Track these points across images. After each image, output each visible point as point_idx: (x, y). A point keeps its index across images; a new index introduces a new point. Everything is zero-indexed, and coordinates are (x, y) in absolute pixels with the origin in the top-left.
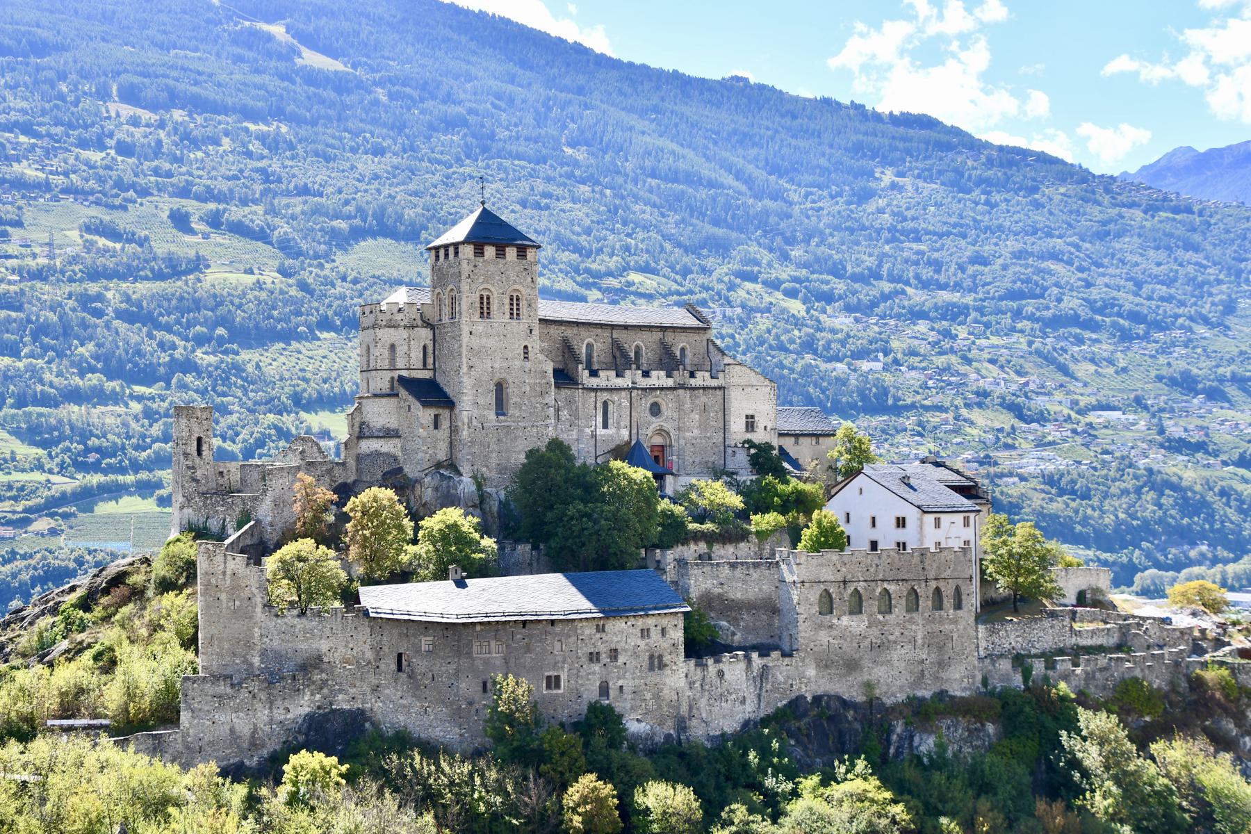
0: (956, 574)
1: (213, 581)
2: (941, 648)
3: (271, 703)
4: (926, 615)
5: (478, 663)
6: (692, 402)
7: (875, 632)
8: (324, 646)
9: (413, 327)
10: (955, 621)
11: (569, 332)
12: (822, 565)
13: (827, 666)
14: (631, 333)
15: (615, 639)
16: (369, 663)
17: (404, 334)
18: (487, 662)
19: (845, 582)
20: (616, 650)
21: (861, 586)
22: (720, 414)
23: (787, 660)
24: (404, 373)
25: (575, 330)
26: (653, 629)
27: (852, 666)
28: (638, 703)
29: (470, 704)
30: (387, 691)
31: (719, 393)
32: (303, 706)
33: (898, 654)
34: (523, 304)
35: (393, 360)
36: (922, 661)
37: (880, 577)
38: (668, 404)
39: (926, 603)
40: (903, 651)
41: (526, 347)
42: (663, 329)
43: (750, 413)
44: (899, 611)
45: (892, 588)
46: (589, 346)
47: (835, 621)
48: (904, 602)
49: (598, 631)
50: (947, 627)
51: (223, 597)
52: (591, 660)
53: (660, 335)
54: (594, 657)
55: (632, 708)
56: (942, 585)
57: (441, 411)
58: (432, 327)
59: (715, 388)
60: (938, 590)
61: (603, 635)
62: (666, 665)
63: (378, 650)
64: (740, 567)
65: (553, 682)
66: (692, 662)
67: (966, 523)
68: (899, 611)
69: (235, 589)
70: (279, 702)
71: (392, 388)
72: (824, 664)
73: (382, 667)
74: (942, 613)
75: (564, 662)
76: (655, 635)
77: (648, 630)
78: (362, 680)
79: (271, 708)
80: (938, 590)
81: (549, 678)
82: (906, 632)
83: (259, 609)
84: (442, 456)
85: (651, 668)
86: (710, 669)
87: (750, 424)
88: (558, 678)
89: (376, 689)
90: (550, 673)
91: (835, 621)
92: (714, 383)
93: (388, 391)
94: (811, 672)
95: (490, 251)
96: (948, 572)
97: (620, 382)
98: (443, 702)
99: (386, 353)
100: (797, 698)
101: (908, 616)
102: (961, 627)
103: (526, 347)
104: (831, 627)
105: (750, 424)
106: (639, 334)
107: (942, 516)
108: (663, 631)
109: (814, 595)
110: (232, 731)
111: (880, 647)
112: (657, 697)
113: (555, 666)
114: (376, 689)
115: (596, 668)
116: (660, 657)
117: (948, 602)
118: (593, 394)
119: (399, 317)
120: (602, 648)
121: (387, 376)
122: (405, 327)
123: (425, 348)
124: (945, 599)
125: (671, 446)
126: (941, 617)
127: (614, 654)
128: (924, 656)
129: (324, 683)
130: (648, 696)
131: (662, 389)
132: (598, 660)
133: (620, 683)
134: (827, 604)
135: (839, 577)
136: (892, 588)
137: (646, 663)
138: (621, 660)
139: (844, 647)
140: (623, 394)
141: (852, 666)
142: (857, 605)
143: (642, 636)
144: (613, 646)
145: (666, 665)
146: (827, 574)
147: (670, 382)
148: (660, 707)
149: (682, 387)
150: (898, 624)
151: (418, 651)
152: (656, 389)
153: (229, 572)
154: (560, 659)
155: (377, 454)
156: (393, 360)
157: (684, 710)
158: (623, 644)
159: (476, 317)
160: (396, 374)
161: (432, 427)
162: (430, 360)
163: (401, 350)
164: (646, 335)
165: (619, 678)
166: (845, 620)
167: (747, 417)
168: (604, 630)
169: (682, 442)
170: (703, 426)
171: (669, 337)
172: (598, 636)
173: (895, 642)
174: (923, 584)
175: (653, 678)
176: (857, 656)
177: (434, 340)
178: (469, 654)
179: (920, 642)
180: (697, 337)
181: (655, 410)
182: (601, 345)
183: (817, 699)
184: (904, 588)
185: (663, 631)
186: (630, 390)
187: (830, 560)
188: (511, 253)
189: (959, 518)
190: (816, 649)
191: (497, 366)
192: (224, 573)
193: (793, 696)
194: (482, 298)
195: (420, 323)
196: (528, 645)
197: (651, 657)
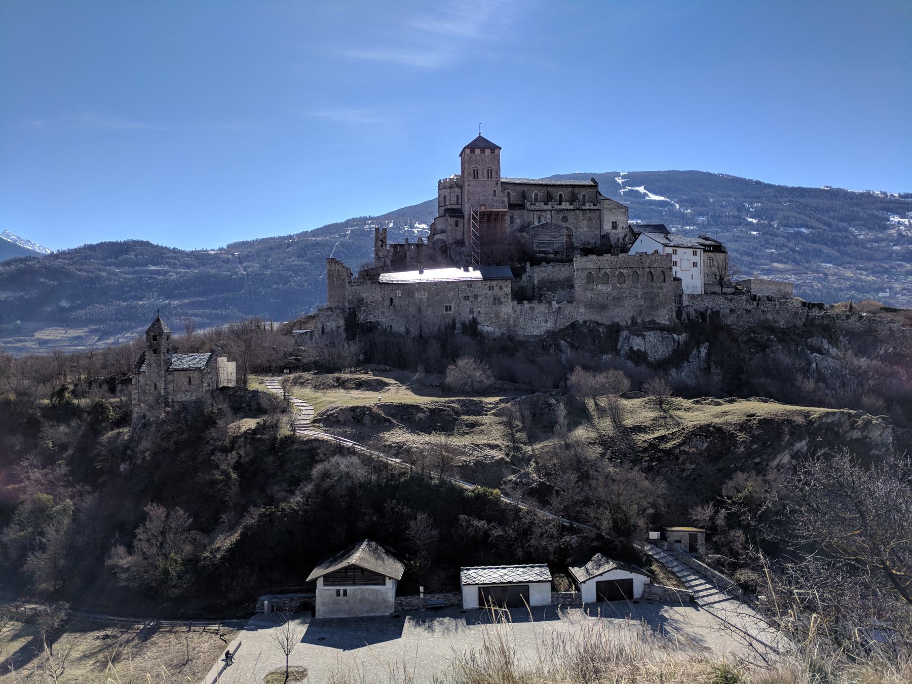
0: (661, 266)
2: (653, 300)
5: (417, 300)
6: (584, 216)
7: (616, 291)
8: (364, 295)
10: (661, 288)
11: (525, 189)
12: (587, 261)
14: (557, 189)
15: (476, 290)
17: (449, 190)
19: (599, 269)
21: (608, 271)
22: (598, 222)
23: (570, 305)
24: (449, 207)
25: (529, 187)
27: (603, 307)
29: (414, 317)
31: (598, 212)
33: (627, 303)
34: (494, 173)
36: (641, 306)
37: (618, 266)
38: (571, 217)
41: (495, 191)
42: (573, 186)
43: (614, 221)
45: (625, 271)
46: (536, 194)
47: (595, 287)
48: (631, 278)
49: (468, 287)
50: (655, 291)
51: (335, 279)
52: (465, 300)
53: (572, 189)
54: (466, 298)
56: (652, 270)
57: (458, 219)
58: (461, 188)
59: (595, 210)
60: (650, 272)
61: (471, 289)
62: (502, 303)
63: (383, 297)
65: (448, 308)
66: (516, 302)
67: (695, 253)
69: (339, 276)
71: (445, 214)
72: (590, 306)
74: (653, 284)
76: (496, 289)
77: (493, 287)
78: (378, 309)
81: (446, 307)
82: (632, 293)
83: (347, 284)
84: (459, 238)
85: (494, 304)
86: (525, 305)
87: (615, 225)
88: (450, 306)
89: (383, 313)
90: (447, 305)
91: (595, 287)
92: (595, 208)
94: (582, 310)
95: (478, 151)
97: (546, 207)
99: (443, 200)
100: (575, 322)
101: (634, 285)
102: (664, 291)
103: (495, 191)
104: (593, 289)
105: (615, 225)
106: (561, 189)
107: (678, 249)
108: (501, 288)
109: (584, 275)
110: (332, 329)
111: (618, 299)
112: (497, 316)
116: (499, 299)
118: (532, 213)
120: (470, 294)
121: (443, 209)
122: (449, 188)
123: (458, 196)
125: (572, 235)
126: (652, 285)
127: (476, 297)
128: (642, 303)
129: (365, 310)
130: (493, 316)
131: (567, 210)
133: (479, 310)
134: (590, 278)
135: (597, 266)
136: (625, 271)
137: (491, 300)
138: (479, 299)
139: (600, 299)
140: (547, 212)
141: (603, 307)
142: (605, 279)
143: (490, 290)
145: (502, 303)
146: (590, 265)
147: (572, 207)
148: (499, 321)
149: (578, 209)
151: (396, 296)
152: (564, 210)
153: (336, 270)
154: (451, 298)
155: (438, 240)
157: (511, 322)
159: (472, 179)
161: (454, 226)
162: (460, 201)
164: (564, 189)
165: (478, 307)
166: (600, 286)
167: (613, 222)
169: (578, 233)
170: (589, 226)
171: (576, 190)
173: (626, 297)
174: (642, 270)
177: (461, 193)
178: (413, 296)
179: (640, 297)
180: (591, 190)
181: (565, 219)
182: (541, 194)
183: (585, 322)
184: (631, 271)
185: (501, 288)
186: (551, 211)
187: (592, 259)
188: (488, 152)
190: (585, 300)
191: (481, 199)
193: (573, 321)
194: (474, 171)
195: (455, 186)
196: (438, 293)
197: (494, 299)
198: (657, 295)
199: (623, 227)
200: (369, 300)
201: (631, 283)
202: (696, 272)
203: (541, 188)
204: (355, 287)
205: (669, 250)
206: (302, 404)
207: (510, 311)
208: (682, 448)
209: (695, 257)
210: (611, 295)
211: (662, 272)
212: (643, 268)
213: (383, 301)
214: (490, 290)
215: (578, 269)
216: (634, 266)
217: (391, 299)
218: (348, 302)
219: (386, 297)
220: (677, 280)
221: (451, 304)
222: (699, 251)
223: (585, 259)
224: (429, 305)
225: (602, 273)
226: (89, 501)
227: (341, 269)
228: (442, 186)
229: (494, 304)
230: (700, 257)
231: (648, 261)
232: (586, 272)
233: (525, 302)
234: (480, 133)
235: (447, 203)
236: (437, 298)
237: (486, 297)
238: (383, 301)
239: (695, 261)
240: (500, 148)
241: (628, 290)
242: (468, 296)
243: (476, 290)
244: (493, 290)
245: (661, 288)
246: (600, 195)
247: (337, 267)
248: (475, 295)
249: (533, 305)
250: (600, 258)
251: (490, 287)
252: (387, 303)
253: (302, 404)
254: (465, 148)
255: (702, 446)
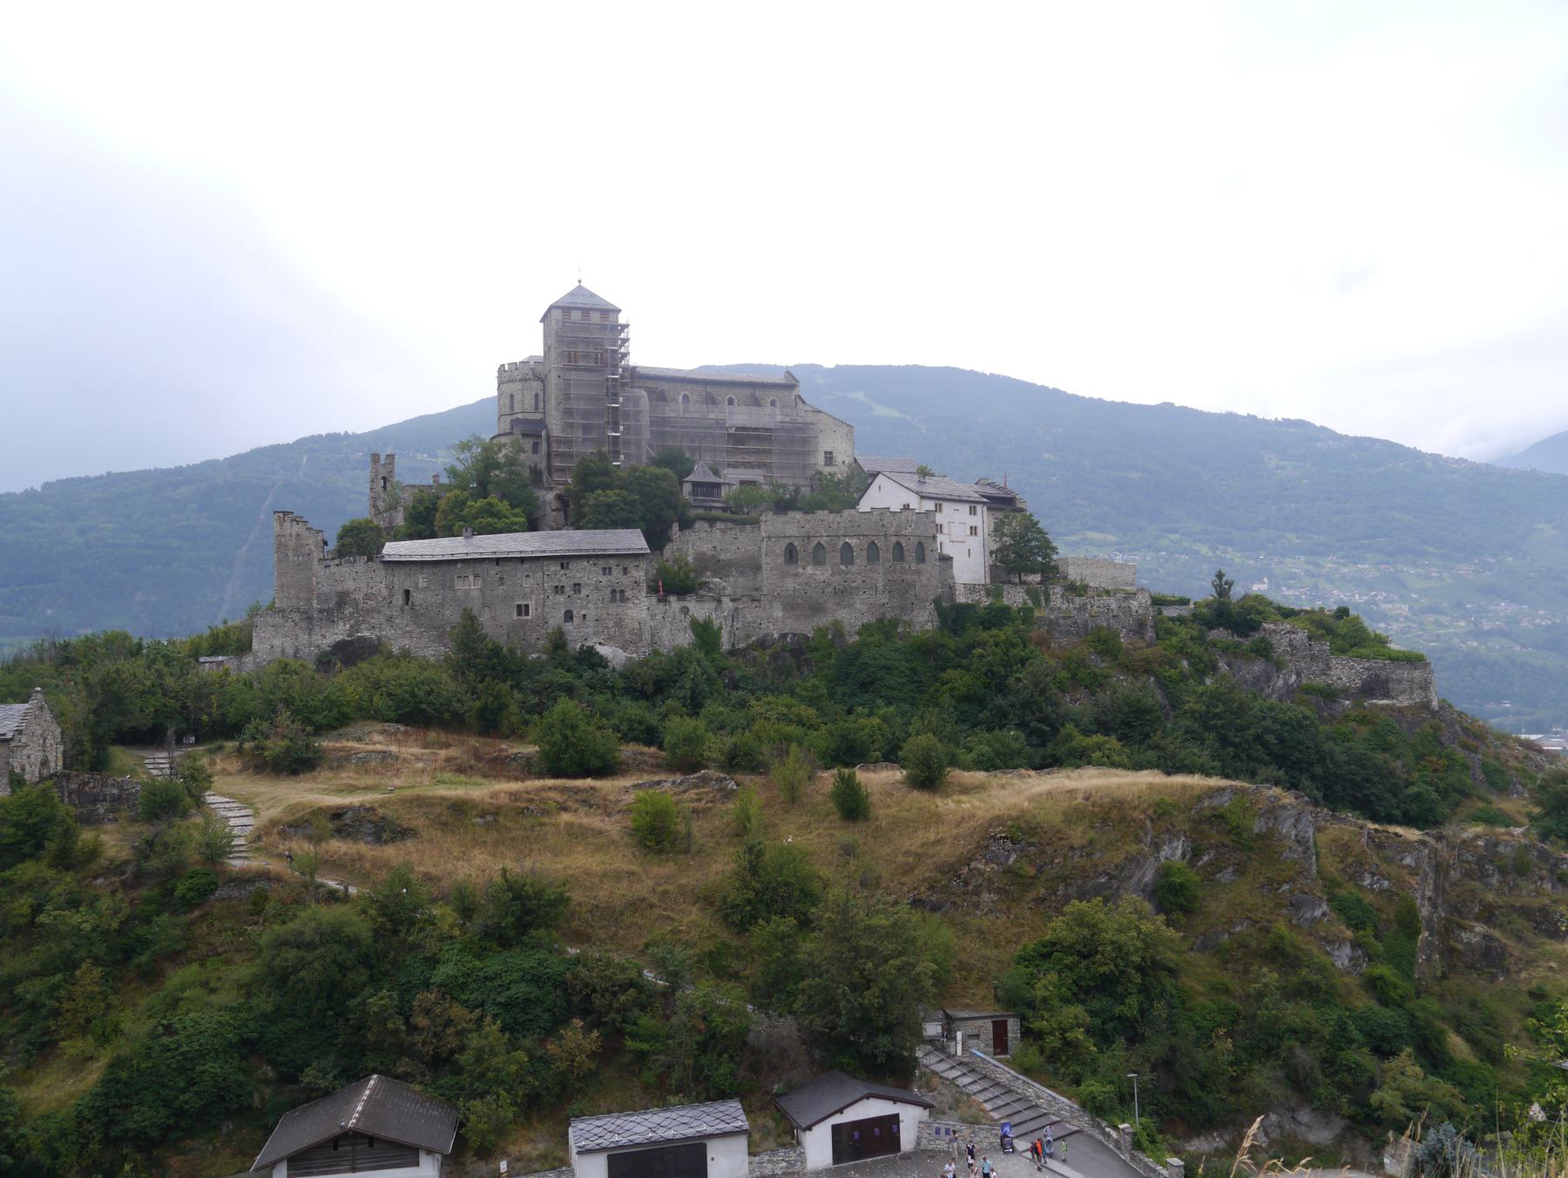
0: (919, 533)
1: (283, 541)
3: (311, 630)
4: (887, 565)
9: (526, 380)
10: (918, 572)
12: (786, 522)
13: (792, 609)
15: (578, 575)
16: (384, 599)
17: (519, 386)
18: (467, 593)
19: (808, 537)
20: (579, 584)
21: (824, 541)
23: (755, 603)
24: (520, 416)
26: (614, 567)
27: (817, 608)
28: (600, 629)
30: (397, 621)
32: (338, 632)
35: (512, 407)
37: (842, 532)
39: (886, 555)
40: (865, 596)
43: (829, 450)
44: (860, 561)
46: (686, 398)
47: (801, 570)
48: (865, 553)
49: (562, 567)
50: (908, 577)
51: (290, 553)
52: (557, 592)
53: (750, 391)
54: (559, 590)
55: (594, 634)
58: (543, 381)
60: (898, 543)
62: (628, 599)
63: (390, 588)
64: (729, 532)
65: (523, 610)
67: (973, 511)
68: (860, 561)
70: (317, 629)
71: (512, 428)
72: (790, 606)
73: (394, 602)
75: (532, 593)
76: (617, 573)
79: (310, 635)
80: (898, 543)
83: (315, 562)
85: (613, 600)
88: (527, 606)
89: (390, 619)
91: (801, 570)
93: (507, 431)
96: (909, 530)
98: (435, 628)
99: (508, 402)
100: (766, 635)
102: (924, 579)
105: (829, 458)
108: (625, 571)
111: (843, 593)
112: (619, 623)
113: (524, 596)
114: (390, 619)
115: (562, 599)
116: (622, 592)
117: (910, 554)
119: (517, 372)
120: (565, 581)
121: (510, 418)
123: (537, 395)
124: (907, 553)
126: (903, 568)
127: (577, 587)
128: (885, 601)
132: (563, 592)
133: (583, 612)
134: (791, 554)
135: (803, 532)
136: (853, 542)
137: (608, 597)
138: (584, 592)
141: (817, 608)
142: (818, 555)
143: (604, 574)
144: (577, 581)
145: (628, 599)
146: (792, 530)
150: (859, 573)
151: (416, 587)
153: (294, 534)
154: (527, 590)
156: (512, 407)
158: (585, 579)
160: (514, 417)
161: (530, 453)
162: (541, 405)
163: (517, 398)
165: (582, 608)
166: (810, 570)
167: (826, 453)
168: (568, 568)
171: (759, 393)
172: (562, 572)
173: (857, 588)
174: (883, 539)
175: (615, 609)
176: (821, 601)
177: (544, 390)
178: (452, 587)
183: (784, 636)
184: (865, 542)
185: (625, 571)
189: (966, 508)
190: (782, 593)
192: (291, 534)
195: (532, 377)
196: (501, 579)
197: (614, 591)
198: (912, 585)
199: (844, 462)
200: (359, 596)
201: (865, 563)
202: (975, 543)
203: (694, 386)
204: (333, 569)
205: (930, 505)
206: (227, 805)
207: (644, 616)
208: (973, 865)
209: (973, 517)
210: (829, 585)
211: (920, 543)
212: (886, 536)
213: (391, 596)
214: (604, 574)
215: (769, 537)
216: (868, 533)
217: (407, 592)
218: (319, 598)
219: (396, 587)
220: (946, 560)
221: (529, 602)
222: (979, 508)
223: (781, 518)
224: (484, 606)
225: (813, 545)
226: (904, 772)
227: (304, 532)
228: (506, 376)
229: (613, 600)
230: (983, 519)
231: (895, 524)
232: (784, 544)
233: (673, 598)
234: (580, 281)
235: (516, 410)
236: (501, 590)
237: (597, 588)
238: (391, 596)
239: (974, 525)
240: (619, 311)
241: (860, 577)
242: (563, 587)
243: (578, 575)
244: (610, 574)
245: (918, 572)
246: (804, 403)
247: (296, 528)
248: (575, 585)
249: (685, 604)
250: (809, 517)
251: (604, 569)
252: (399, 599)
253: (227, 805)
254: (551, 308)
255: (1008, 858)
